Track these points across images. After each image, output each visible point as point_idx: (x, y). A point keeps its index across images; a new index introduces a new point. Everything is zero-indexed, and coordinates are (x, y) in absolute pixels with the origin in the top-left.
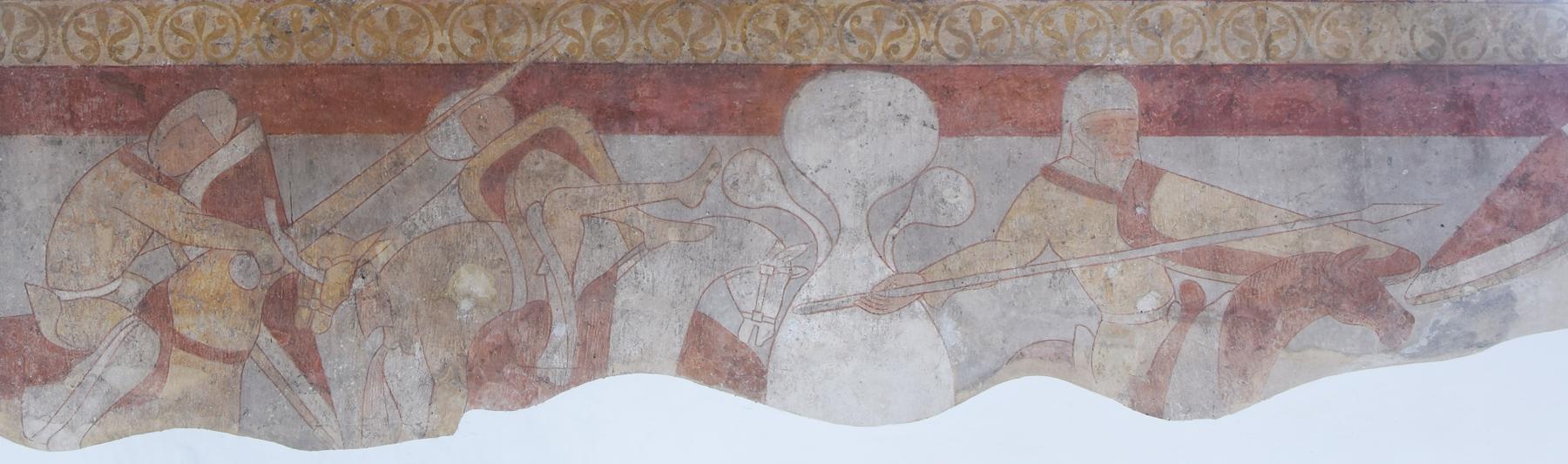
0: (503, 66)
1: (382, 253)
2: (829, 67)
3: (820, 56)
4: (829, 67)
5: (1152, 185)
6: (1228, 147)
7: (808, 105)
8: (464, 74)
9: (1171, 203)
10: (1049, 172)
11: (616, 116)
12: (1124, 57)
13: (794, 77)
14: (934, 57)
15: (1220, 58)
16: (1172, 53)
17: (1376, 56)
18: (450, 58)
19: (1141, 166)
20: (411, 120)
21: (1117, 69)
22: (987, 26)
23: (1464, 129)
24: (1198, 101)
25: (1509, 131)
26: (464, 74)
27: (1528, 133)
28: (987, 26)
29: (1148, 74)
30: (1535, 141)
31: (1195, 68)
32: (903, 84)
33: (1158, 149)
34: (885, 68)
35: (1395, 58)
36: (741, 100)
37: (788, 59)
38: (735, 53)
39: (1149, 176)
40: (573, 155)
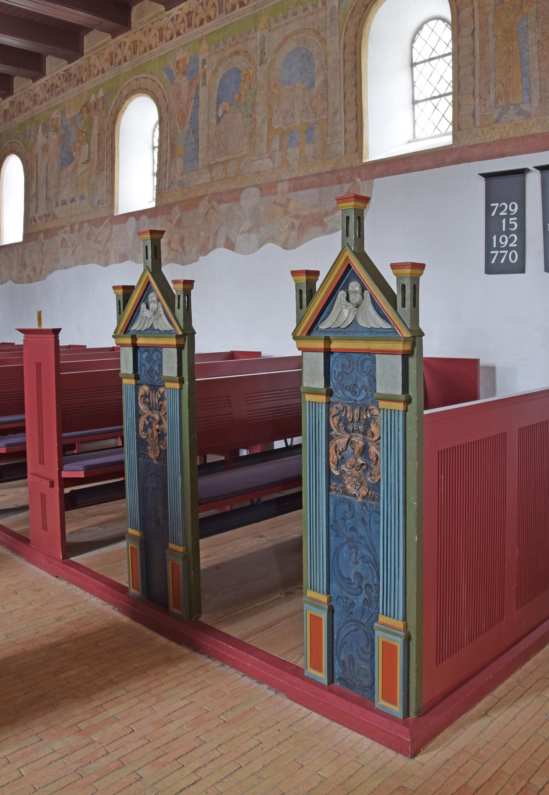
0: (207, 195)
1: (193, 230)
2: (246, 187)
3: (245, 186)
4: (246, 187)
5: (289, 202)
6: (301, 193)
7: (243, 195)
8: (203, 197)
9: (292, 206)
10: (275, 202)
11: (220, 202)
12: (287, 178)
13: (242, 189)
14: (260, 183)
15: (301, 175)
16: (294, 176)
17: (325, 170)
18: (202, 195)
19: (288, 199)
20: (197, 206)
21: (285, 180)
22: (267, 175)
23: (340, 183)
24: (298, 184)
25: (347, 182)
26: (203, 197)
27: (350, 182)
28: (267, 175)
29: (290, 180)
30: (351, 184)
31: (297, 178)
32: (256, 189)
33: (291, 195)
34: (253, 186)
35: (329, 170)
36: (234, 196)
37: (241, 187)
38: (235, 187)
39: (289, 200)
40: (215, 209)
